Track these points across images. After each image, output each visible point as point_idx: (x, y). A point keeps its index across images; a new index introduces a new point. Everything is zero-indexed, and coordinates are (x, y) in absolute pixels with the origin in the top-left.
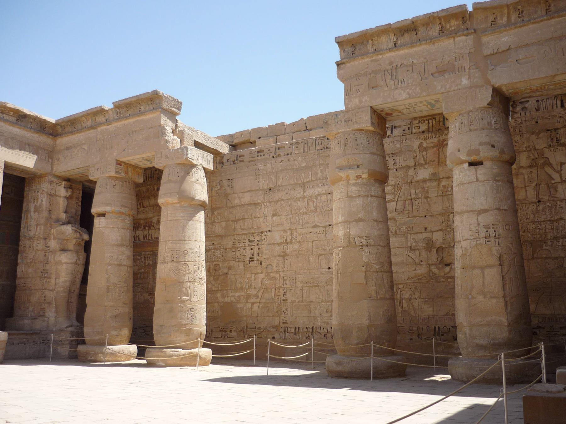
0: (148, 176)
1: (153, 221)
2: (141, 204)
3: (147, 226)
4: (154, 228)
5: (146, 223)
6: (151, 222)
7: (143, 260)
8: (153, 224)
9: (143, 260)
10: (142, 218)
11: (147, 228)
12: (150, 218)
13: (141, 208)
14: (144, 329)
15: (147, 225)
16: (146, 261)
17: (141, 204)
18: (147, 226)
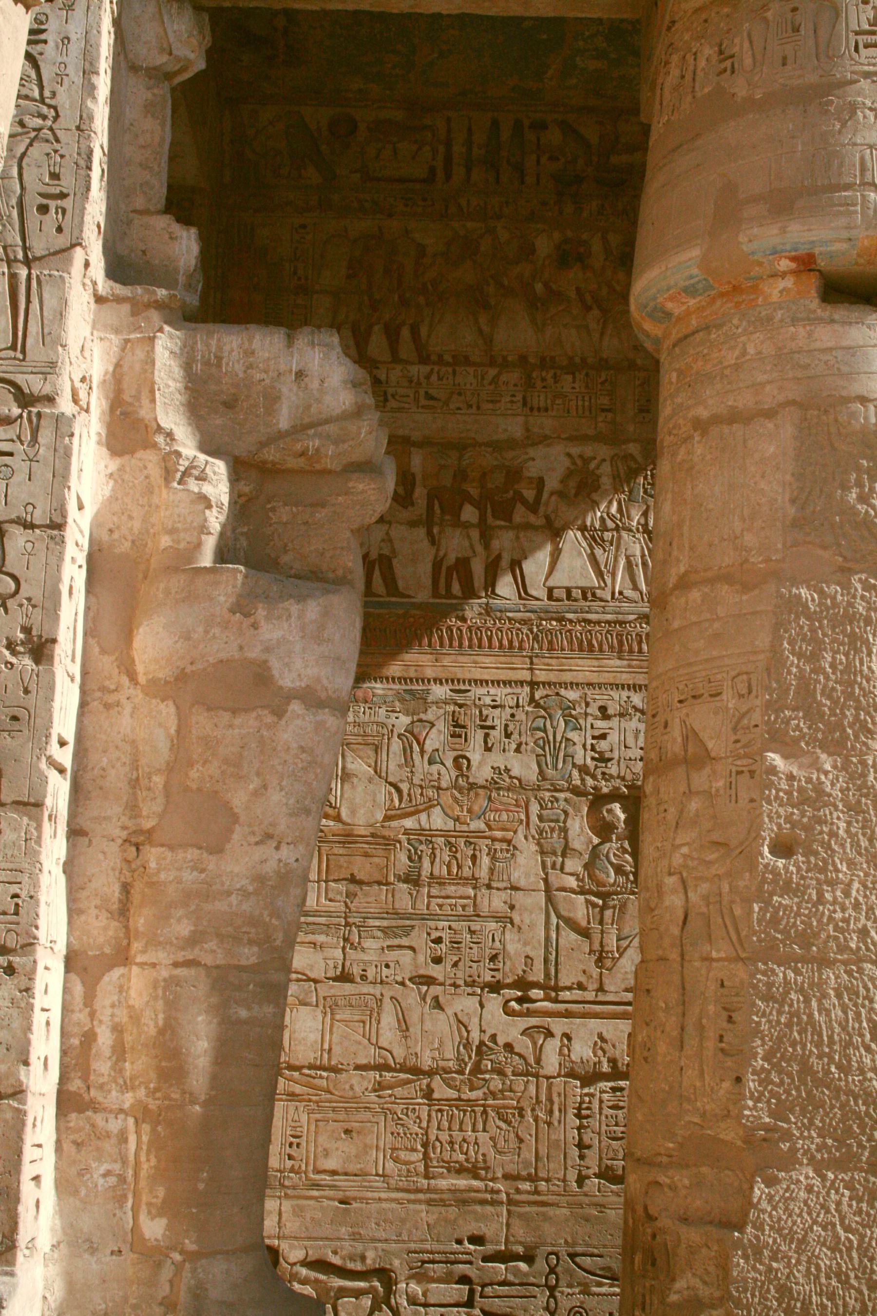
0: (458, 149)
1: (533, 470)
2: (405, 333)
3: (467, 498)
4: (532, 519)
5: (461, 475)
6: (514, 475)
7: (435, 739)
8: (529, 494)
9: (435, 739)
10: (416, 436)
11: (469, 513)
12: (496, 446)
13: (396, 359)
14: (464, 1279)
15: (474, 492)
16: (475, 755)
17: (405, 333)
18: (467, 498)
